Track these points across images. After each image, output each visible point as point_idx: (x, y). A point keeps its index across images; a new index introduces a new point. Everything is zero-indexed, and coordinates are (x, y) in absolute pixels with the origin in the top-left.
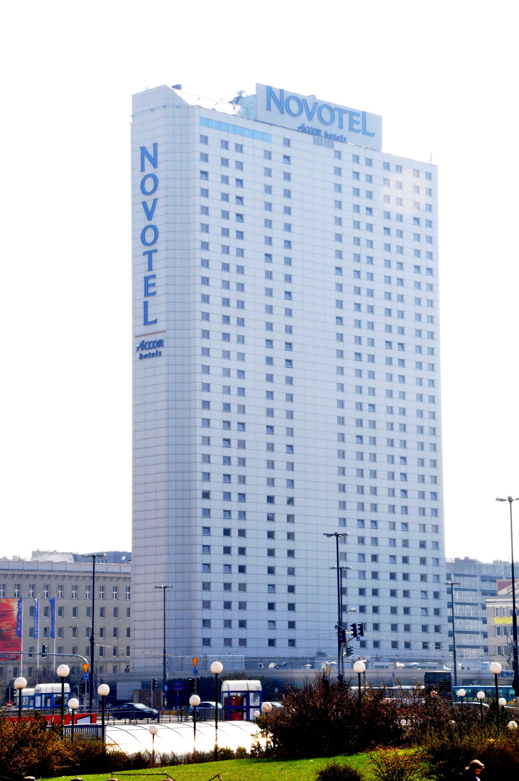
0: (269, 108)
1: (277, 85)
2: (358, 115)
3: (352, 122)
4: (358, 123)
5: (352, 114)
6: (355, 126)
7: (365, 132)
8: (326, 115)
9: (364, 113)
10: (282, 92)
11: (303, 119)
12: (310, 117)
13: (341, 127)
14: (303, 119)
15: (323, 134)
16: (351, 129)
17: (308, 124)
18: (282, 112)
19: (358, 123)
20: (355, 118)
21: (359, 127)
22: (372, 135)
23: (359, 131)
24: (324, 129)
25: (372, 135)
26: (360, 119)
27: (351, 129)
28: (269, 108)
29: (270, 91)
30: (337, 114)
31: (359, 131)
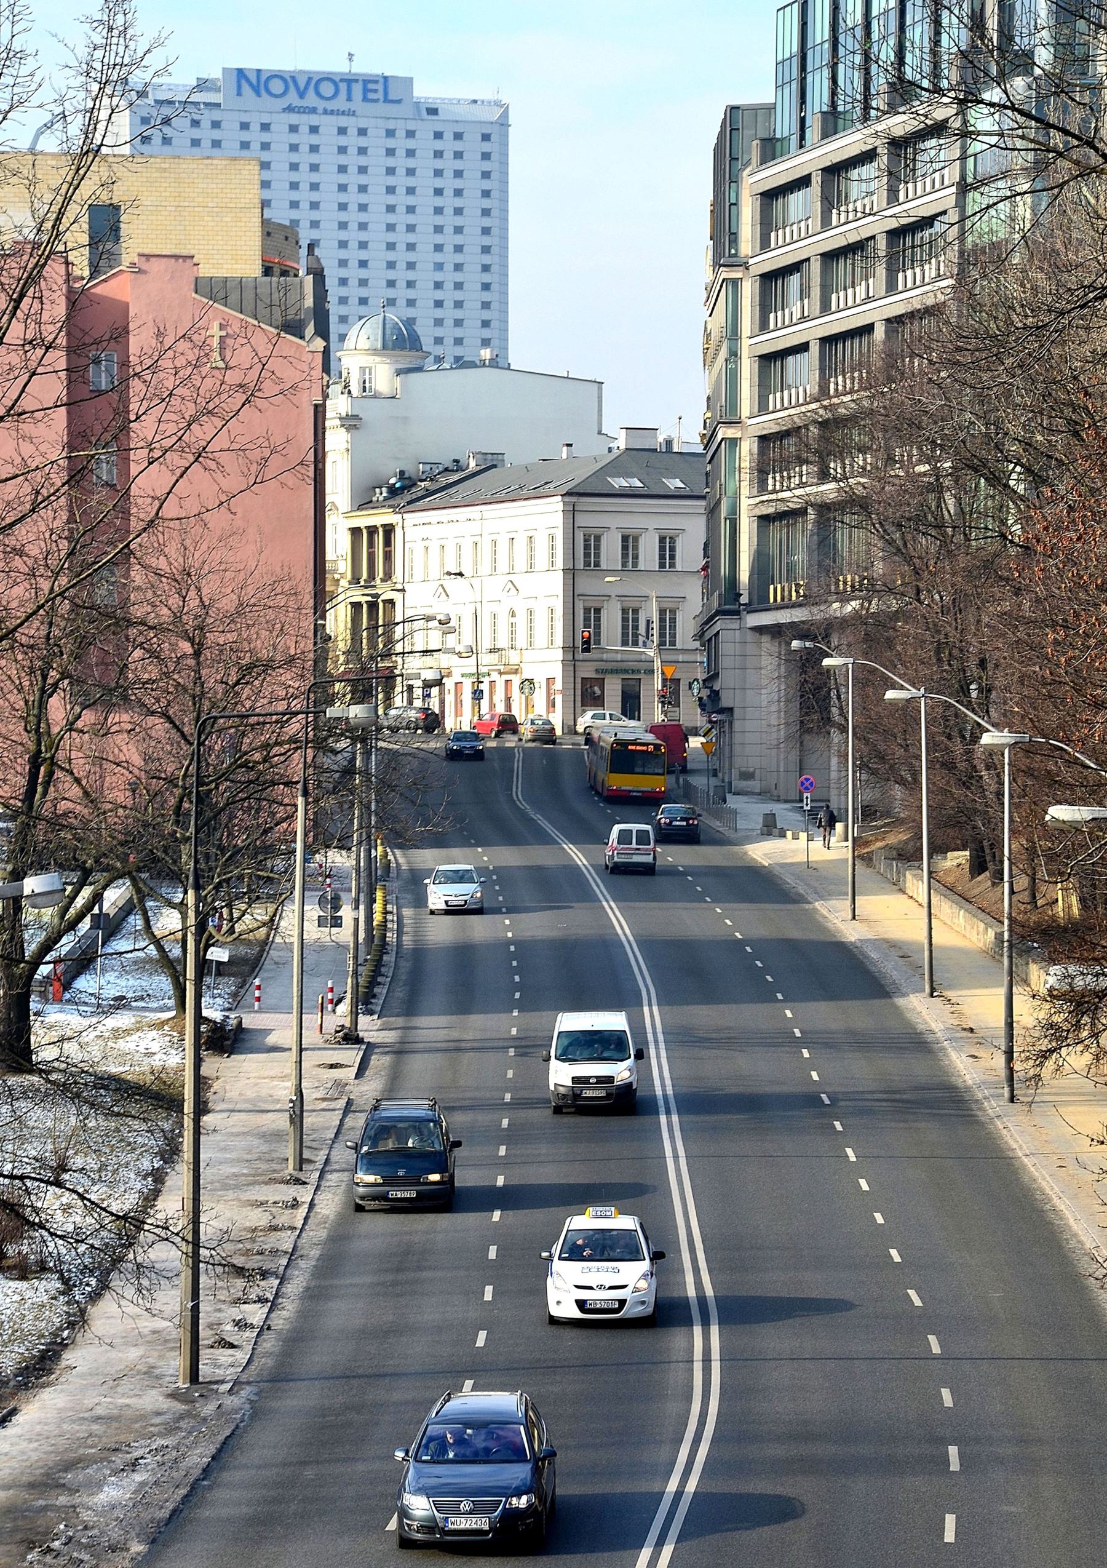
0: (239, 94)
1: (250, 63)
2: (376, 82)
3: (366, 91)
4: (376, 91)
5: (366, 82)
6: (371, 96)
7: (386, 100)
8: (327, 89)
9: (386, 78)
10: (259, 71)
11: (292, 98)
12: (302, 95)
13: (349, 99)
14: (292, 98)
15: (320, 111)
16: (365, 99)
17: (297, 102)
18: (259, 95)
19: (376, 91)
20: (371, 86)
21: (380, 95)
22: (399, 101)
23: (377, 101)
24: (321, 105)
25: (399, 101)
26: (380, 87)
27: (365, 99)
28: (239, 94)
29: (240, 72)
30: (343, 87)
31: (377, 101)
